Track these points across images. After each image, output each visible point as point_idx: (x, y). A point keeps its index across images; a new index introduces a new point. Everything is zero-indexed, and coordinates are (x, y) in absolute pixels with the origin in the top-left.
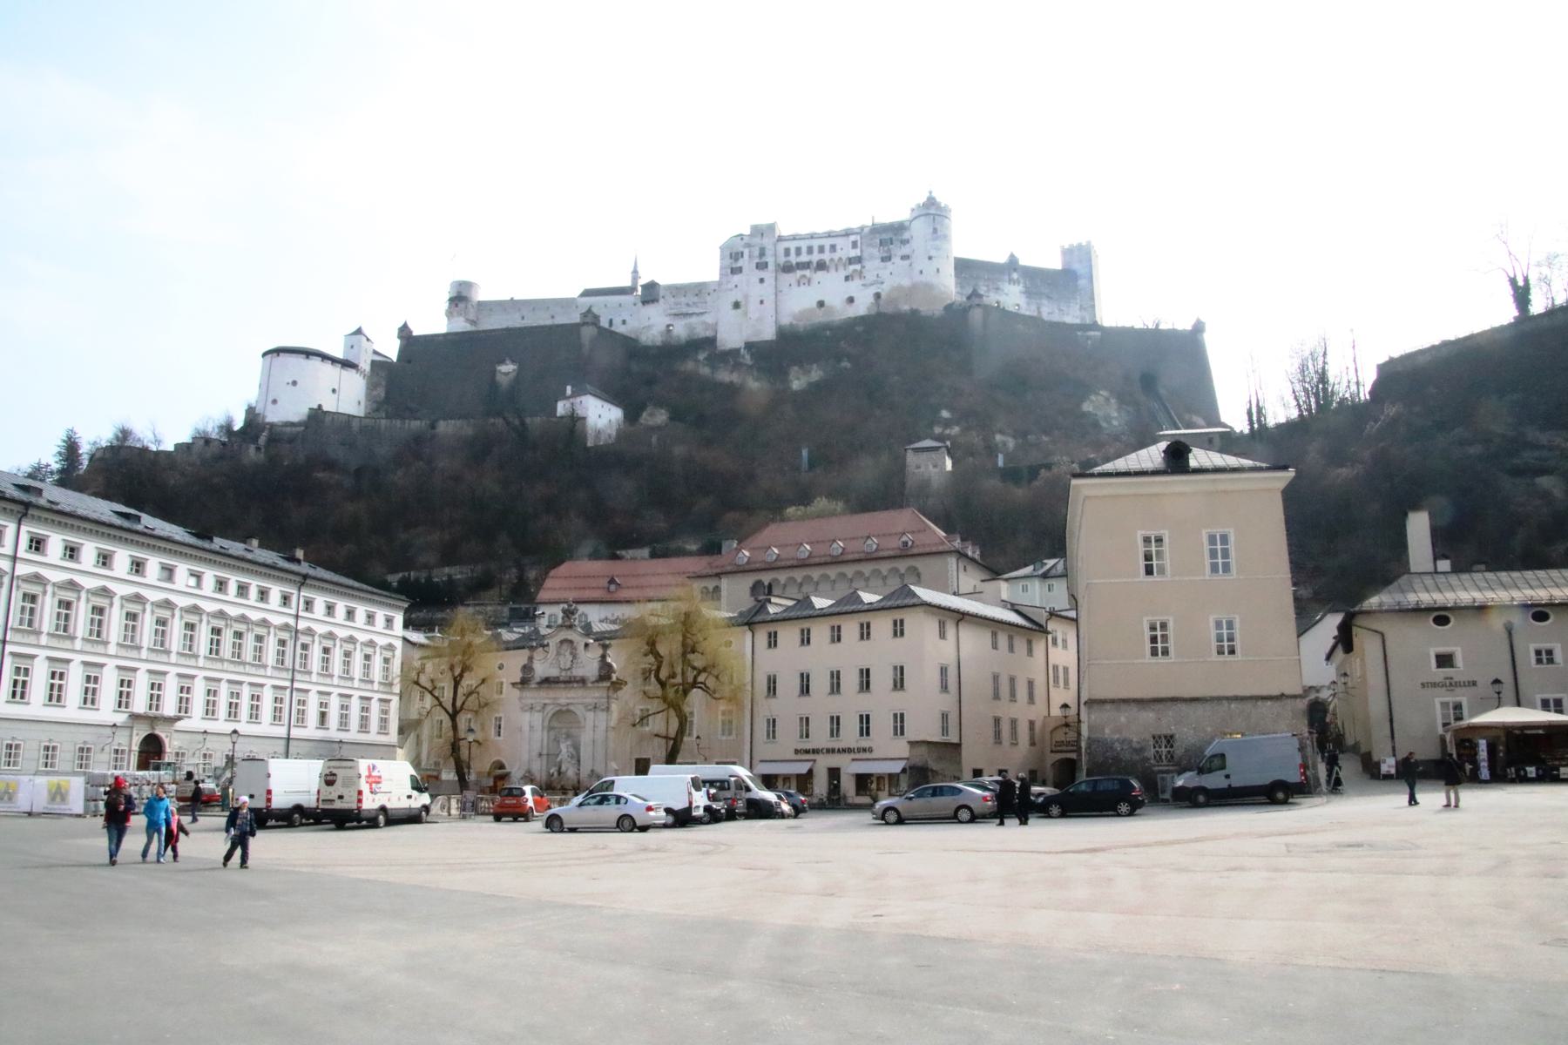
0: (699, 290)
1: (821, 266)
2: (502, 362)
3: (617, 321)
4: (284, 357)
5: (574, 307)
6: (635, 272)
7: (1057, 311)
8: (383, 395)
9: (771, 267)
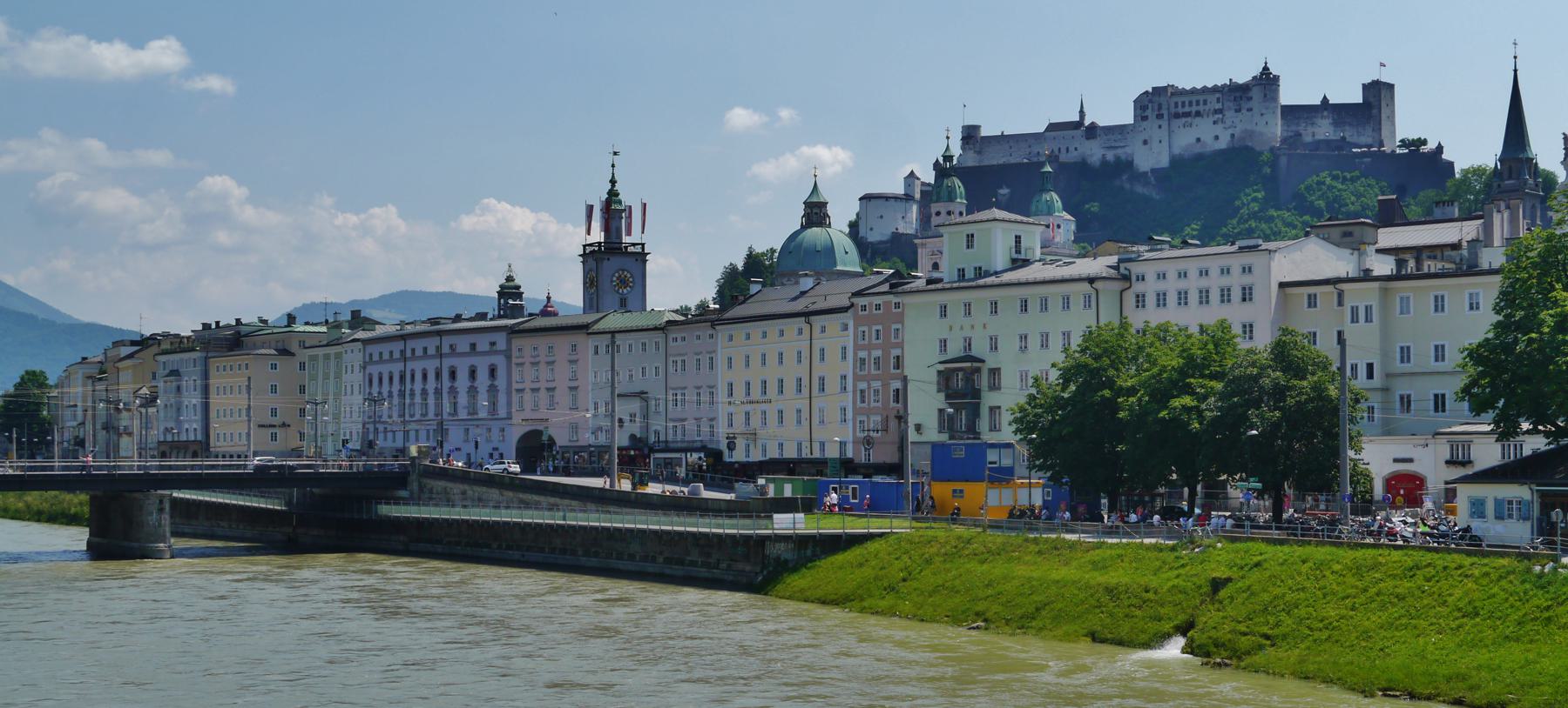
0: (1120, 129)
1: (1198, 114)
2: (1001, 188)
4: (873, 202)
6: (1082, 113)
7: (1355, 133)
9: (1166, 117)
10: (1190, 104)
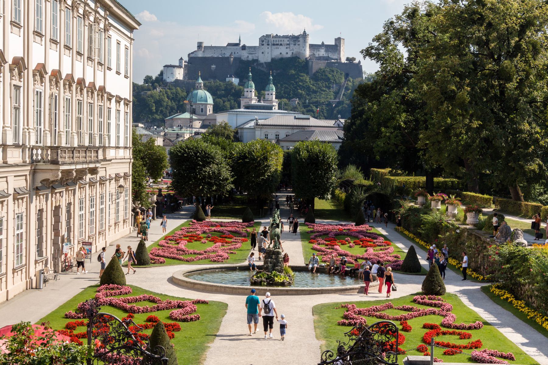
0: (254, 48)
1: (281, 45)
2: (212, 65)
3: (236, 53)
4: (169, 68)
6: (240, 40)
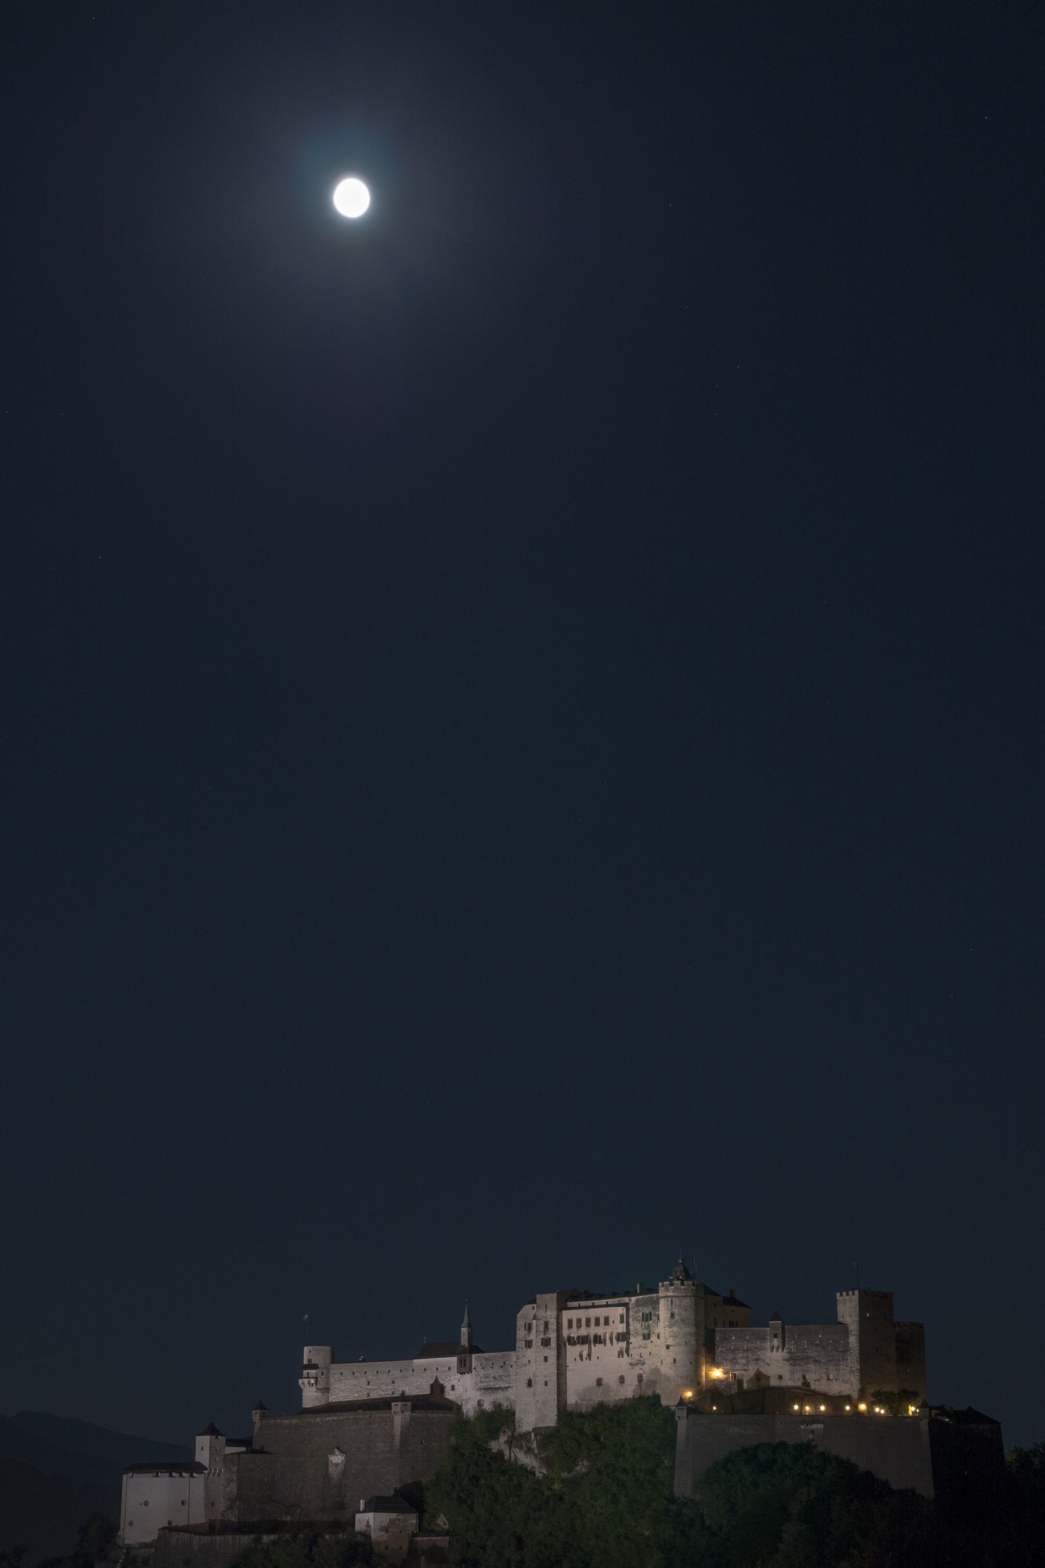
1: (598, 1340)
2: (332, 1453)
5: (411, 1370)
8: (235, 1490)
9: (553, 1344)
10: (588, 1320)
